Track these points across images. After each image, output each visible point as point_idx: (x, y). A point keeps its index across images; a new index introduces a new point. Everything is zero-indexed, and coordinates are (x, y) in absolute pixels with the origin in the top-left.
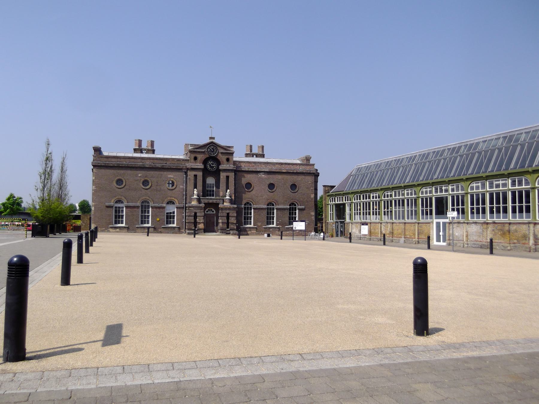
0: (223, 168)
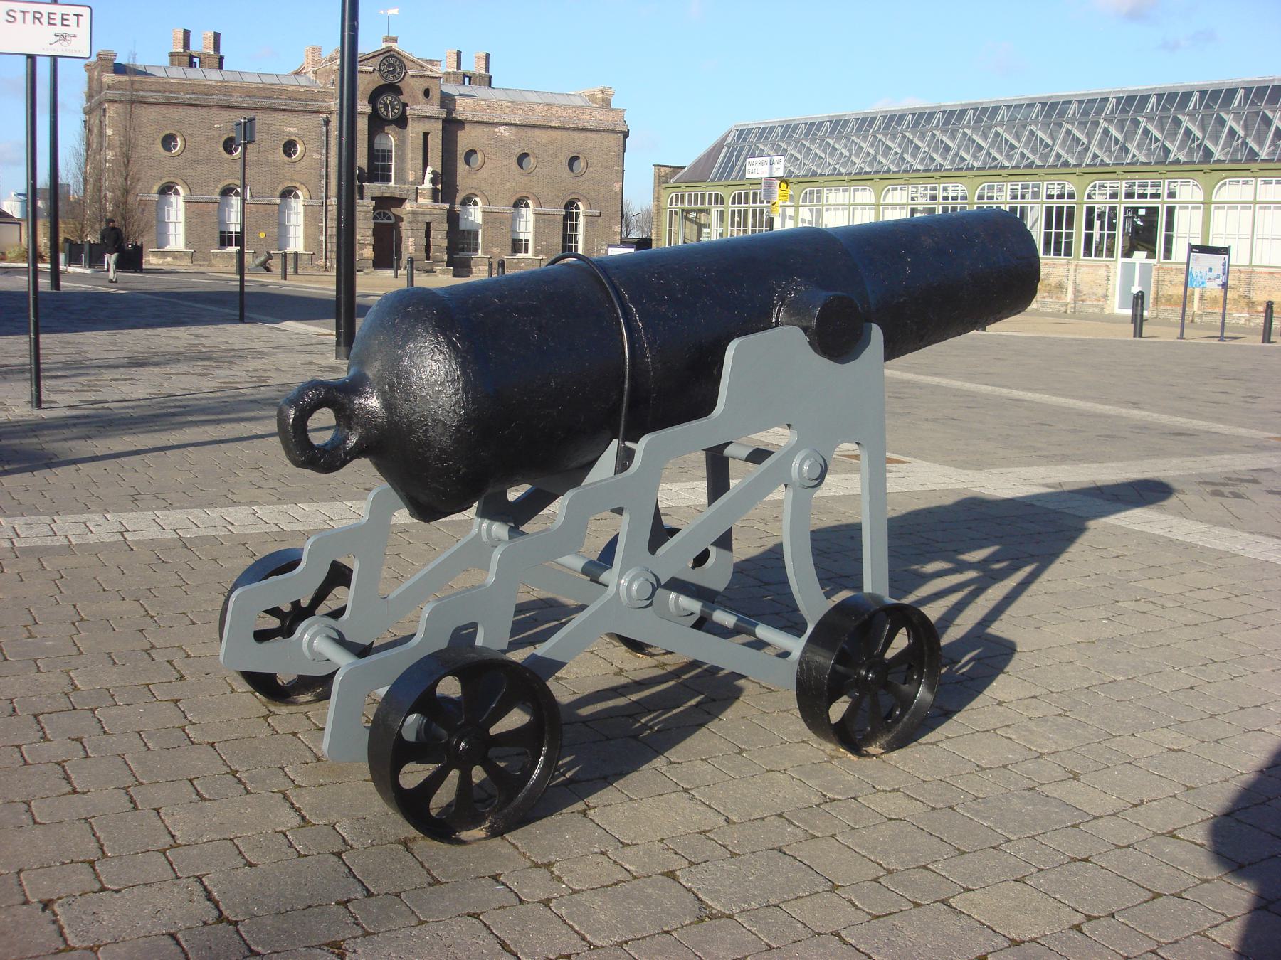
0: (417, 113)
